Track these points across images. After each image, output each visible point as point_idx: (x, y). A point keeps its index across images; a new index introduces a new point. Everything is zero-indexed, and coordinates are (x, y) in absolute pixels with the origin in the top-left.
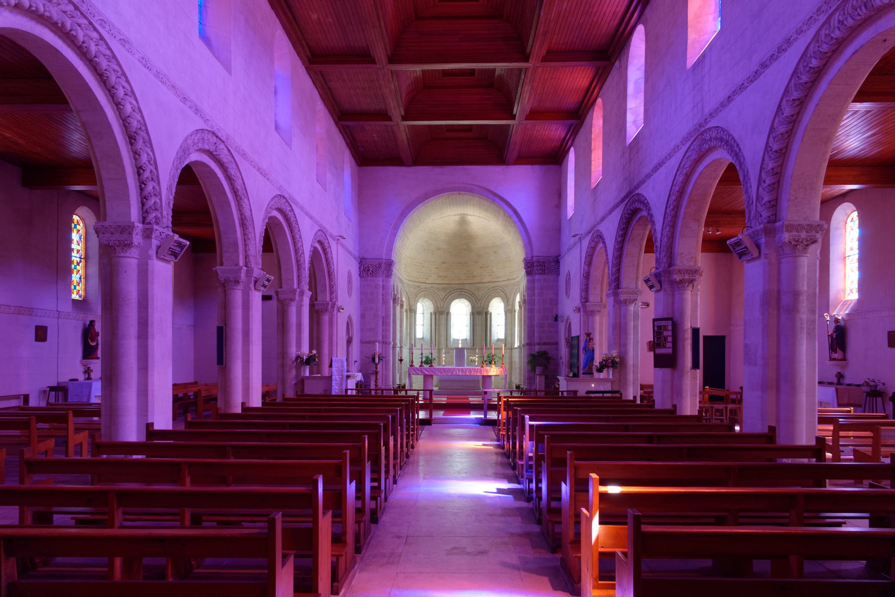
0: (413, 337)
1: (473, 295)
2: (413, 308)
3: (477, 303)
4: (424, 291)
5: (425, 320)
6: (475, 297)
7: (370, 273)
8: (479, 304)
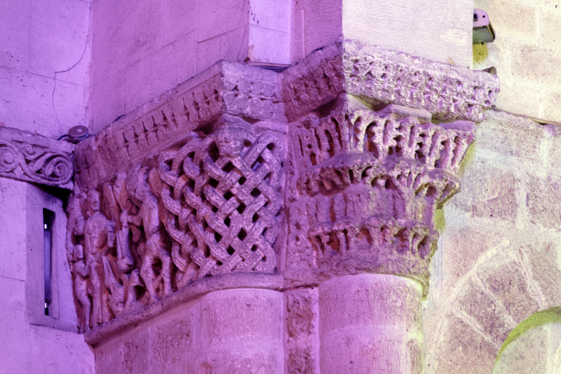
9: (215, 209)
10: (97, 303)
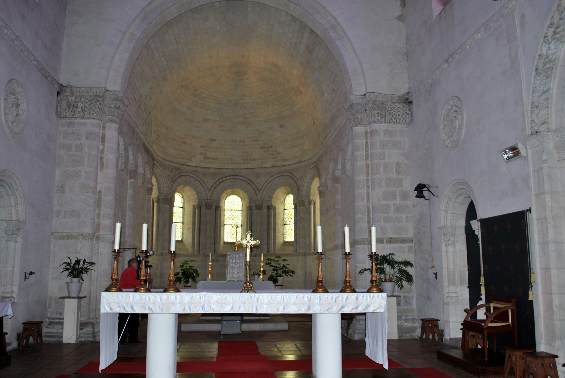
1: (251, 184)
3: (257, 195)
5: (185, 216)
6: (254, 186)
10: (62, 114)
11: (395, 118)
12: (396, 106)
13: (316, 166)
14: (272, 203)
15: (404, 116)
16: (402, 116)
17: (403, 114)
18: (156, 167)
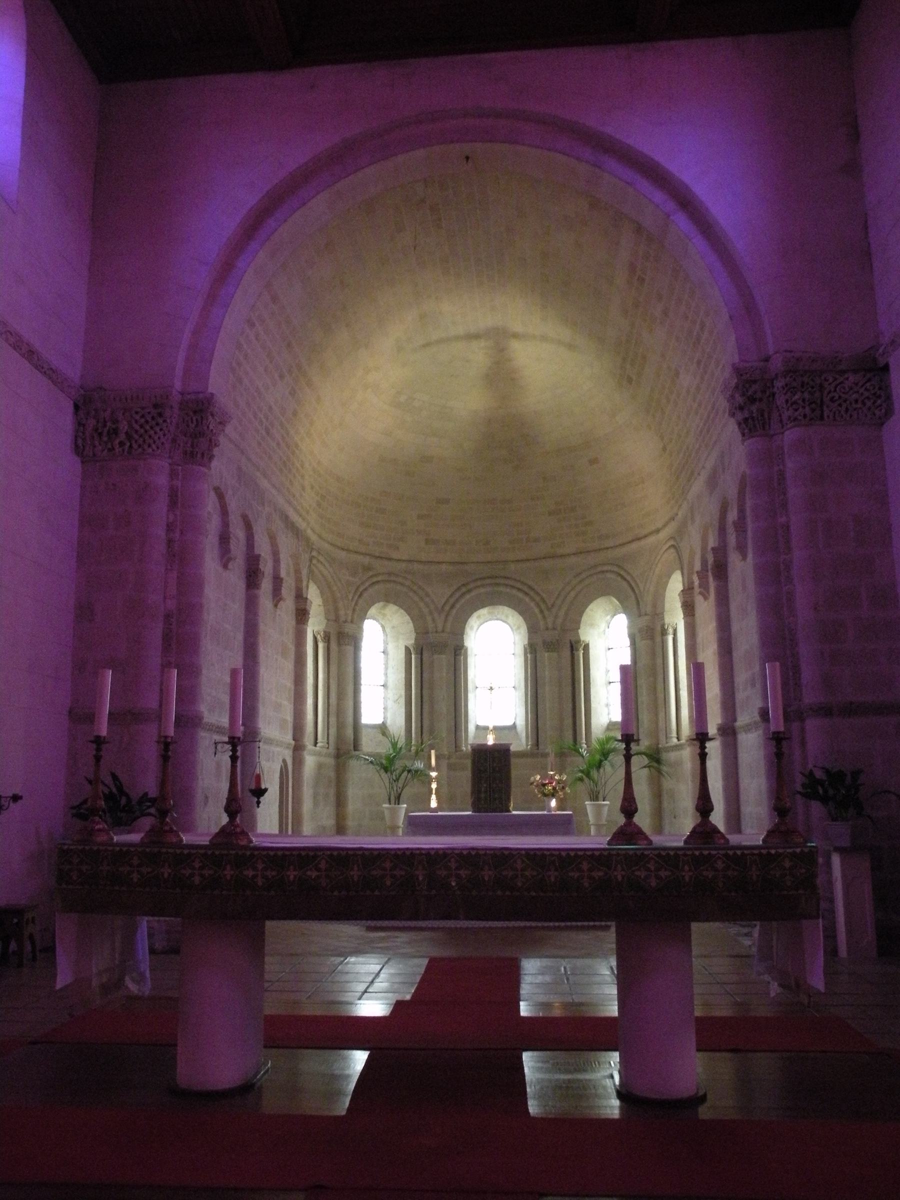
0: (350, 719)
2: (349, 628)
3: (544, 617)
4: (384, 581)
5: (390, 671)
7: (121, 444)
8: (550, 621)
9: (156, 433)
10: (87, 448)
11: (847, 410)
12: (847, 379)
13: (673, 546)
14: (579, 636)
15: (869, 403)
16: (864, 404)
17: (868, 398)
18: (319, 565)
